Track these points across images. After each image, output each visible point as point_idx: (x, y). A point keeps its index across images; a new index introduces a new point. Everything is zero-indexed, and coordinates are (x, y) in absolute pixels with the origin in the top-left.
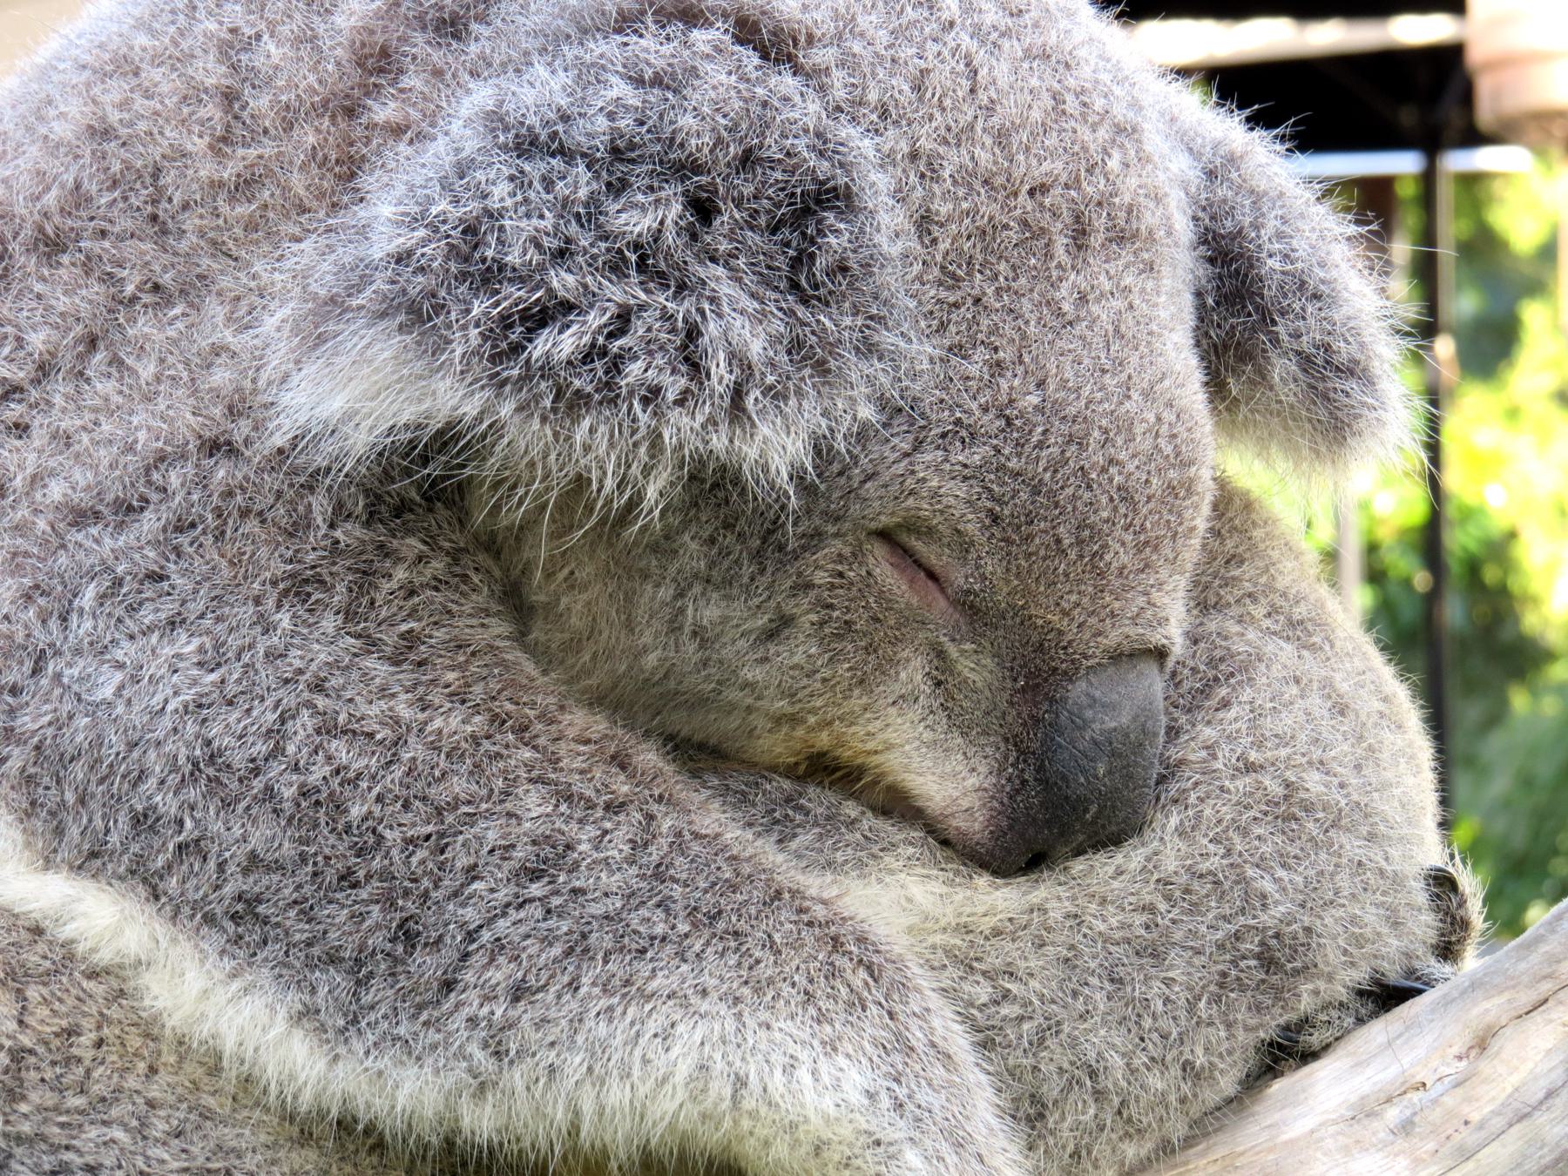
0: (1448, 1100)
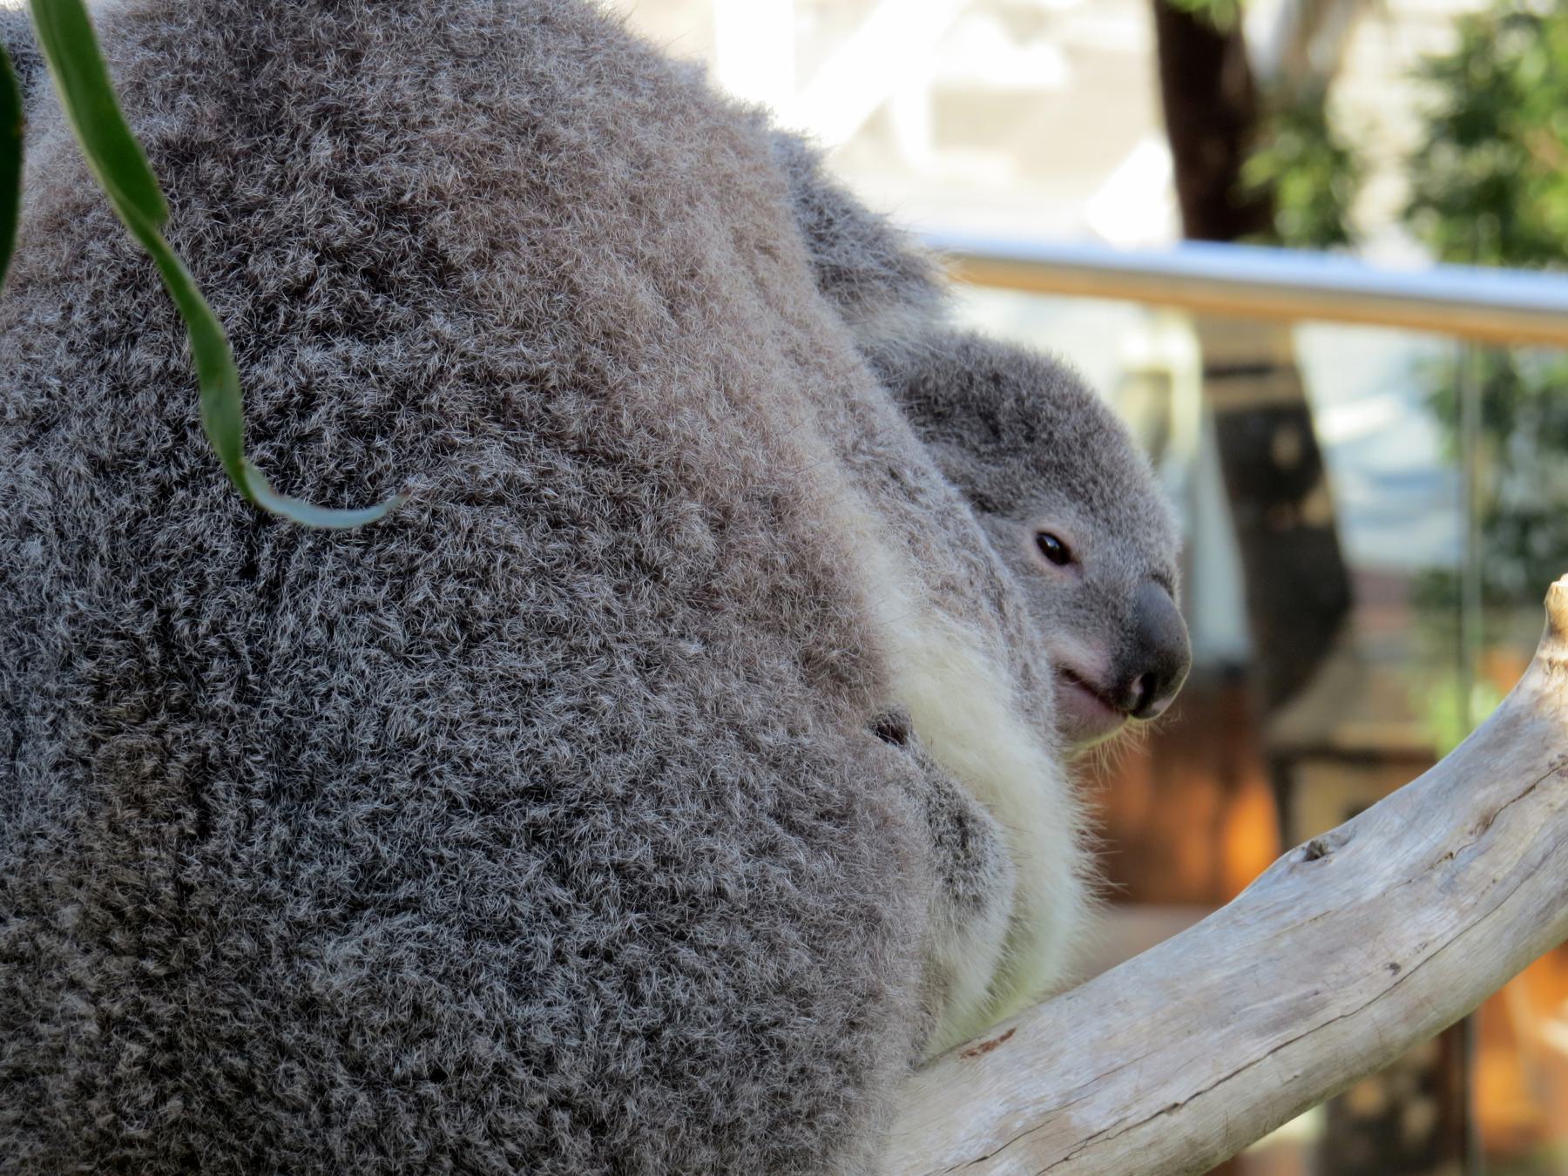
0: (1479, 865)
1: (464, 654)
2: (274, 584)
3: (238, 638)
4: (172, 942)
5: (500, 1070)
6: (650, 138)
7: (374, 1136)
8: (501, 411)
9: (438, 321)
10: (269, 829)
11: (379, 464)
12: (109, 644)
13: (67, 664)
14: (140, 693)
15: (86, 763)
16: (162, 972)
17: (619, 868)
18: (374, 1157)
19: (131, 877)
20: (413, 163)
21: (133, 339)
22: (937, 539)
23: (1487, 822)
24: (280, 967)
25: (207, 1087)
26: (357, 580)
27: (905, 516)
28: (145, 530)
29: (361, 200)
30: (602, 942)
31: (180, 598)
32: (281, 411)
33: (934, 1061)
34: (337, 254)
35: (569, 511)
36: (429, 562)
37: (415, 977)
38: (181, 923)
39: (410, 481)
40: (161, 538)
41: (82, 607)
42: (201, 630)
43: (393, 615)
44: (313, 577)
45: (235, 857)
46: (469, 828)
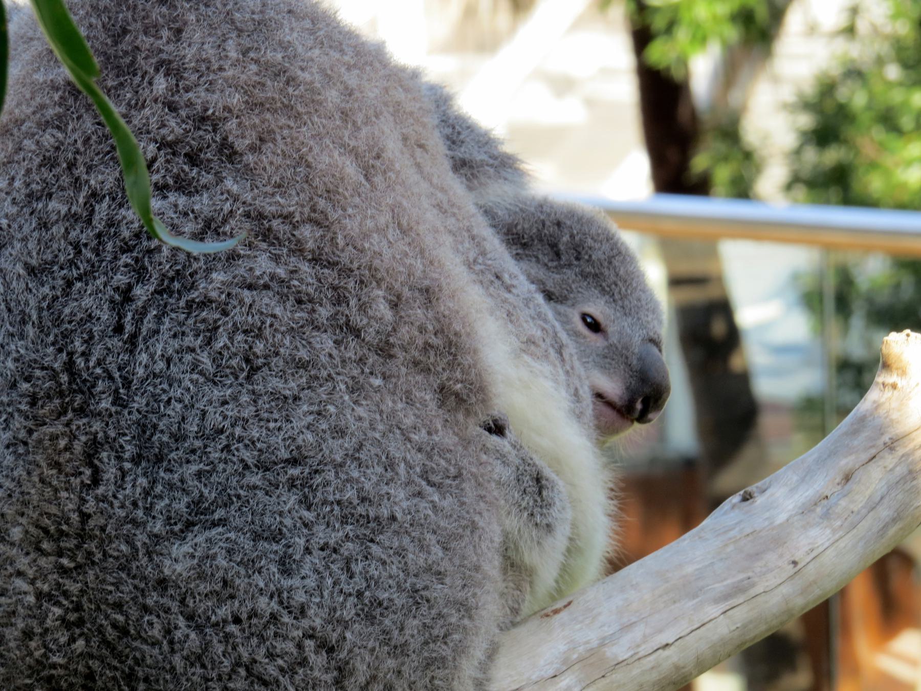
0: (843, 503)
1: (248, 378)
2: (134, 337)
3: (113, 368)
4: (78, 547)
5: (274, 617)
6: (352, 79)
7: (199, 657)
8: (267, 235)
9: (229, 184)
10: (135, 480)
11: (195, 266)
12: (38, 373)
13: (14, 385)
14: (57, 401)
15: (25, 444)
16: (72, 565)
17: (339, 503)
18: (199, 671)
19: (53, 510)
20: (214, 92)
21: (50, 196)
22: (524, 314)
23: (847, 478)
24: (144, 561)
25: (100, 632)
26: (183, 333)
27: (505, 301)
28: (57, 306)
29: (183, 113)
30: (332, 542)
31: (78, 345)
32: (137, 236)
33: (525, 621)
34: (169, 145)
35: (308, 294)
36: (225, 324)
37: (224, 563)
38: (83, 536)
39: (214, 275)
40: (67, 311)
41: (22, 351)
42: (91, 364)
43: (205, 354)
44: (157, 332)
45: (115, 497)
46: (255, 479)
